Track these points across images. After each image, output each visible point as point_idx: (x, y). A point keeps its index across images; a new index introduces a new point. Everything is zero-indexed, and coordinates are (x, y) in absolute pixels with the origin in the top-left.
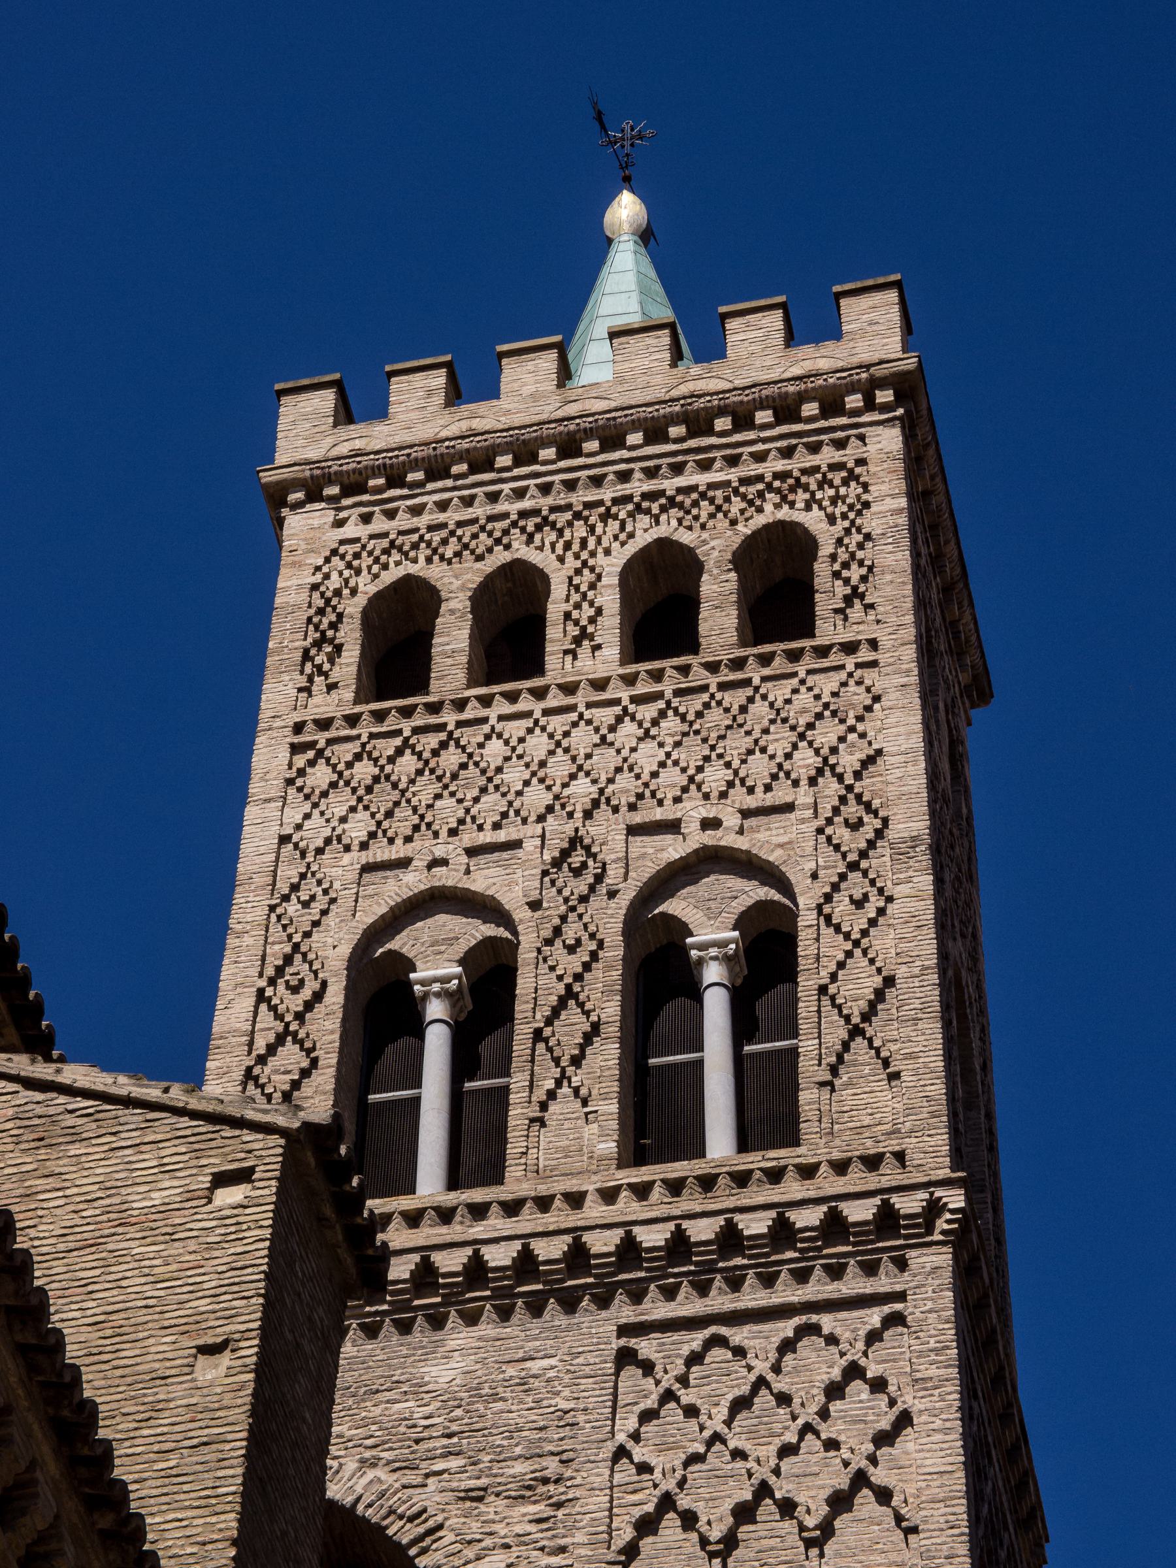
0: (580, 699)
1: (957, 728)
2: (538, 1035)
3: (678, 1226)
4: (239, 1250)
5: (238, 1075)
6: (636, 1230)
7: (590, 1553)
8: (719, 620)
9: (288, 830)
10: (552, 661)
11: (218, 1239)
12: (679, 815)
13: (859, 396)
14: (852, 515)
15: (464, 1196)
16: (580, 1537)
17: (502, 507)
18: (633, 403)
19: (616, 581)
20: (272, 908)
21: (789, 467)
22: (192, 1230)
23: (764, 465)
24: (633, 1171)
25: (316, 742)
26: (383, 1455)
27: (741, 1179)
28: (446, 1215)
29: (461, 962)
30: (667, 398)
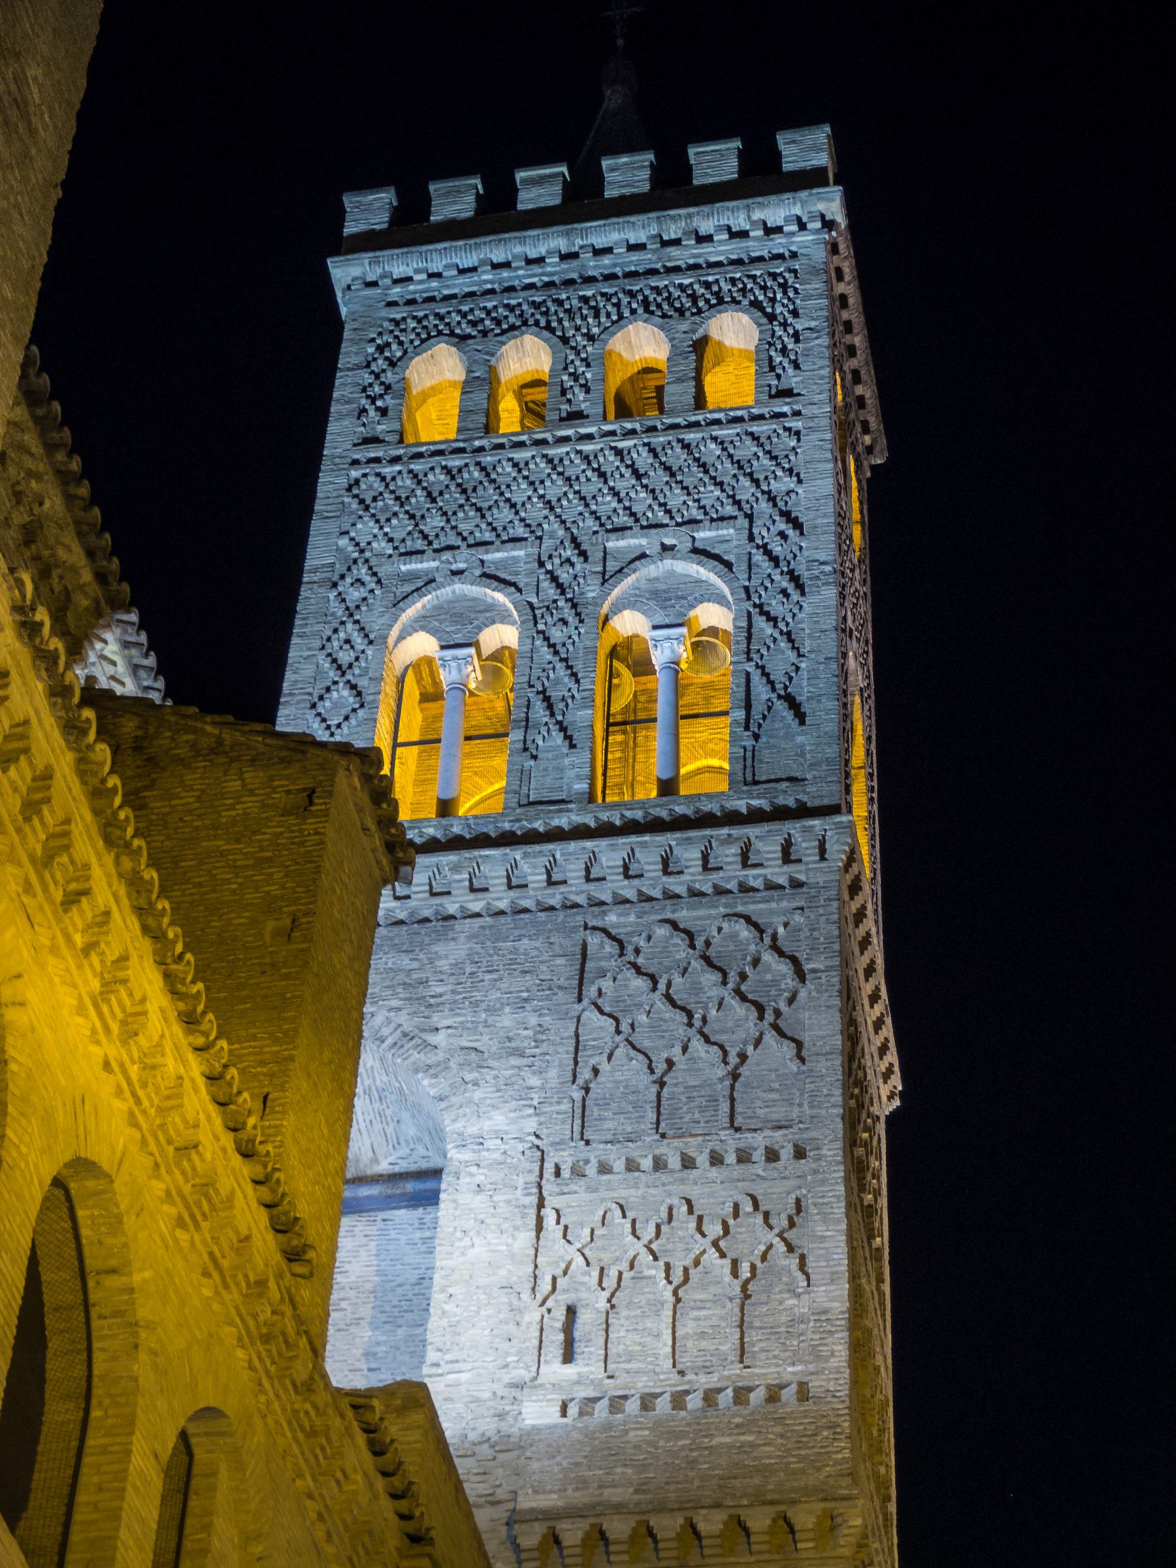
22: (265, 833)
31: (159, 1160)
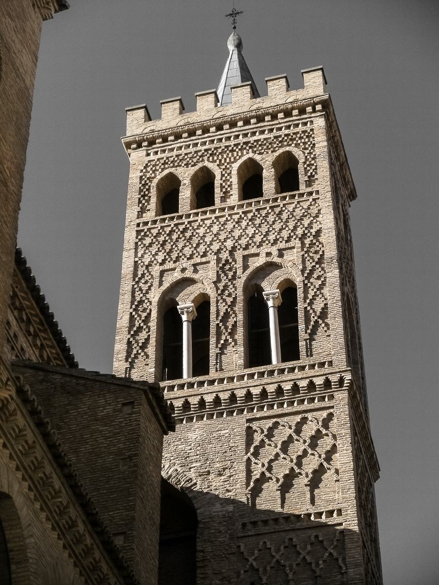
0: (226, 212)
1: (346, 210)
2: (218, 325)
3: (263, 387)
4: (131, 428)
5: (125, 341)
6: (251, 389)
7: (241, 491)
8: (269, 186)
9: (137, 259)
10: (217, 200)
11: (124, 425)
12: (259, 251)
13: (311, 108)
14: (310, 148)
15: (197, 379)
16: (238, 486)
17: (199, 147)
18: (239, 112)
19: (236, 172)
20: (133, 285)
21: (290, 132)
22: (116, 422)
23: (281, 132)
24: (249, 369)
25: (144, 230)
26: (176, 462)
27: (282, 371)
28: (191, 385)
29: (193, 302)
30: (251, 109)
31: (87, 577)
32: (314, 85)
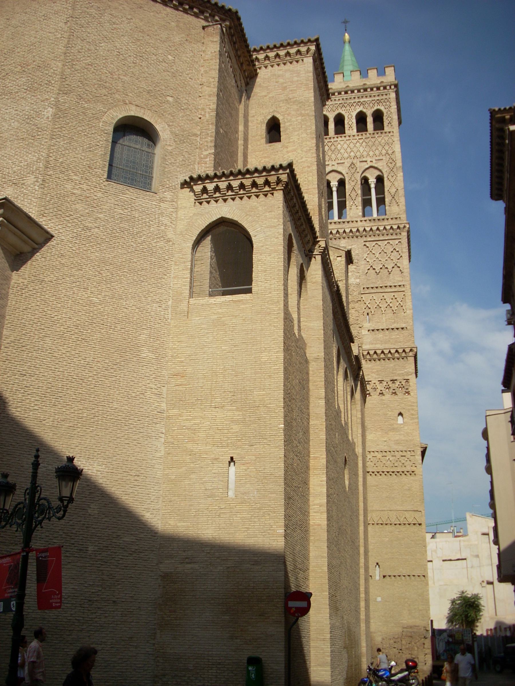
0: (351, 138)
10: (346, 132)
16: (361, 271)
17: (336, 102)
29: (338, 182)
32: (390, 76)
